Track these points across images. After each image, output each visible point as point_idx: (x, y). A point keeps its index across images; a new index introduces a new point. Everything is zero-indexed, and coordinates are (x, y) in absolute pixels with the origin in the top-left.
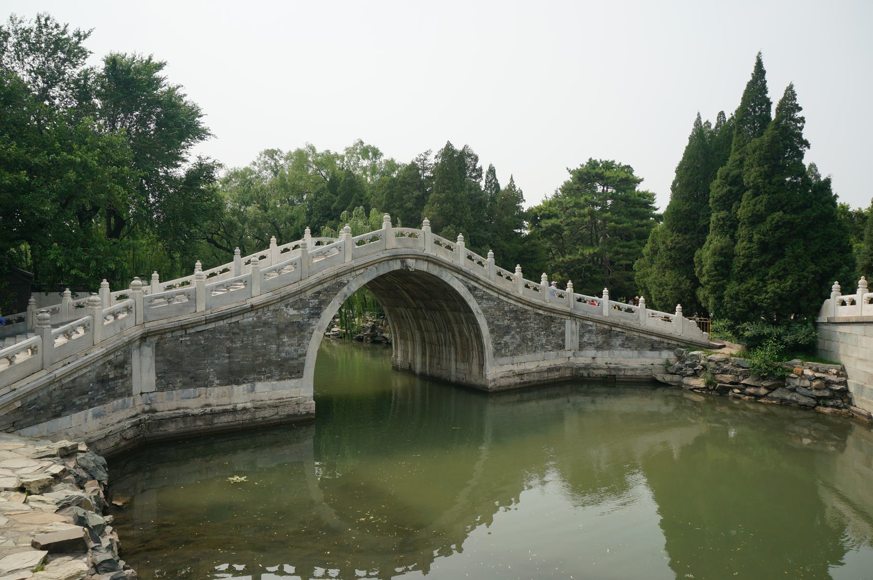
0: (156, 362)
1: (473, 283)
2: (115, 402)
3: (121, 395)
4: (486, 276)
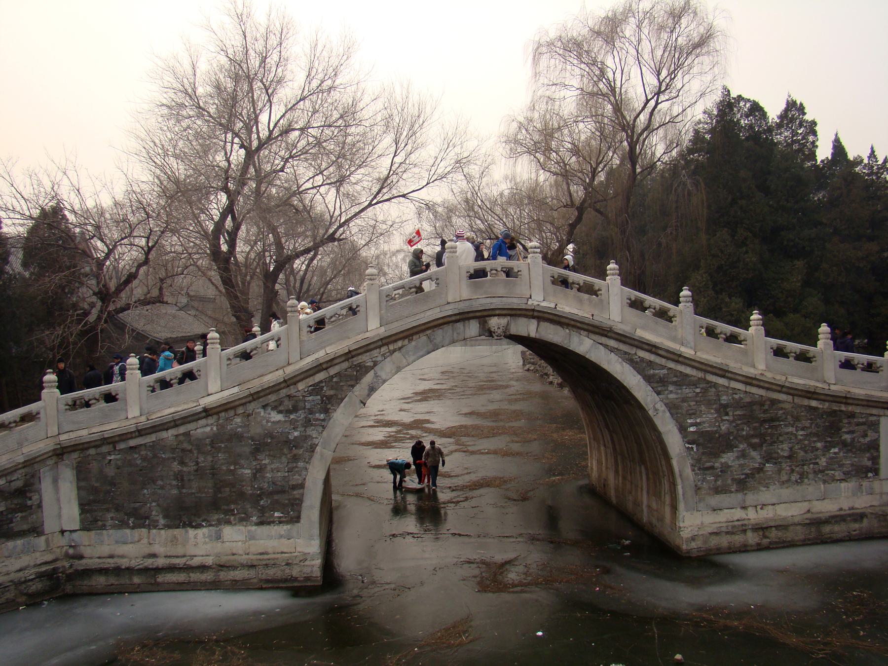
0: (79, 488)
1: (642, 354)
2: (10, 544)
3: (22, 534)
4: (674, 339)
